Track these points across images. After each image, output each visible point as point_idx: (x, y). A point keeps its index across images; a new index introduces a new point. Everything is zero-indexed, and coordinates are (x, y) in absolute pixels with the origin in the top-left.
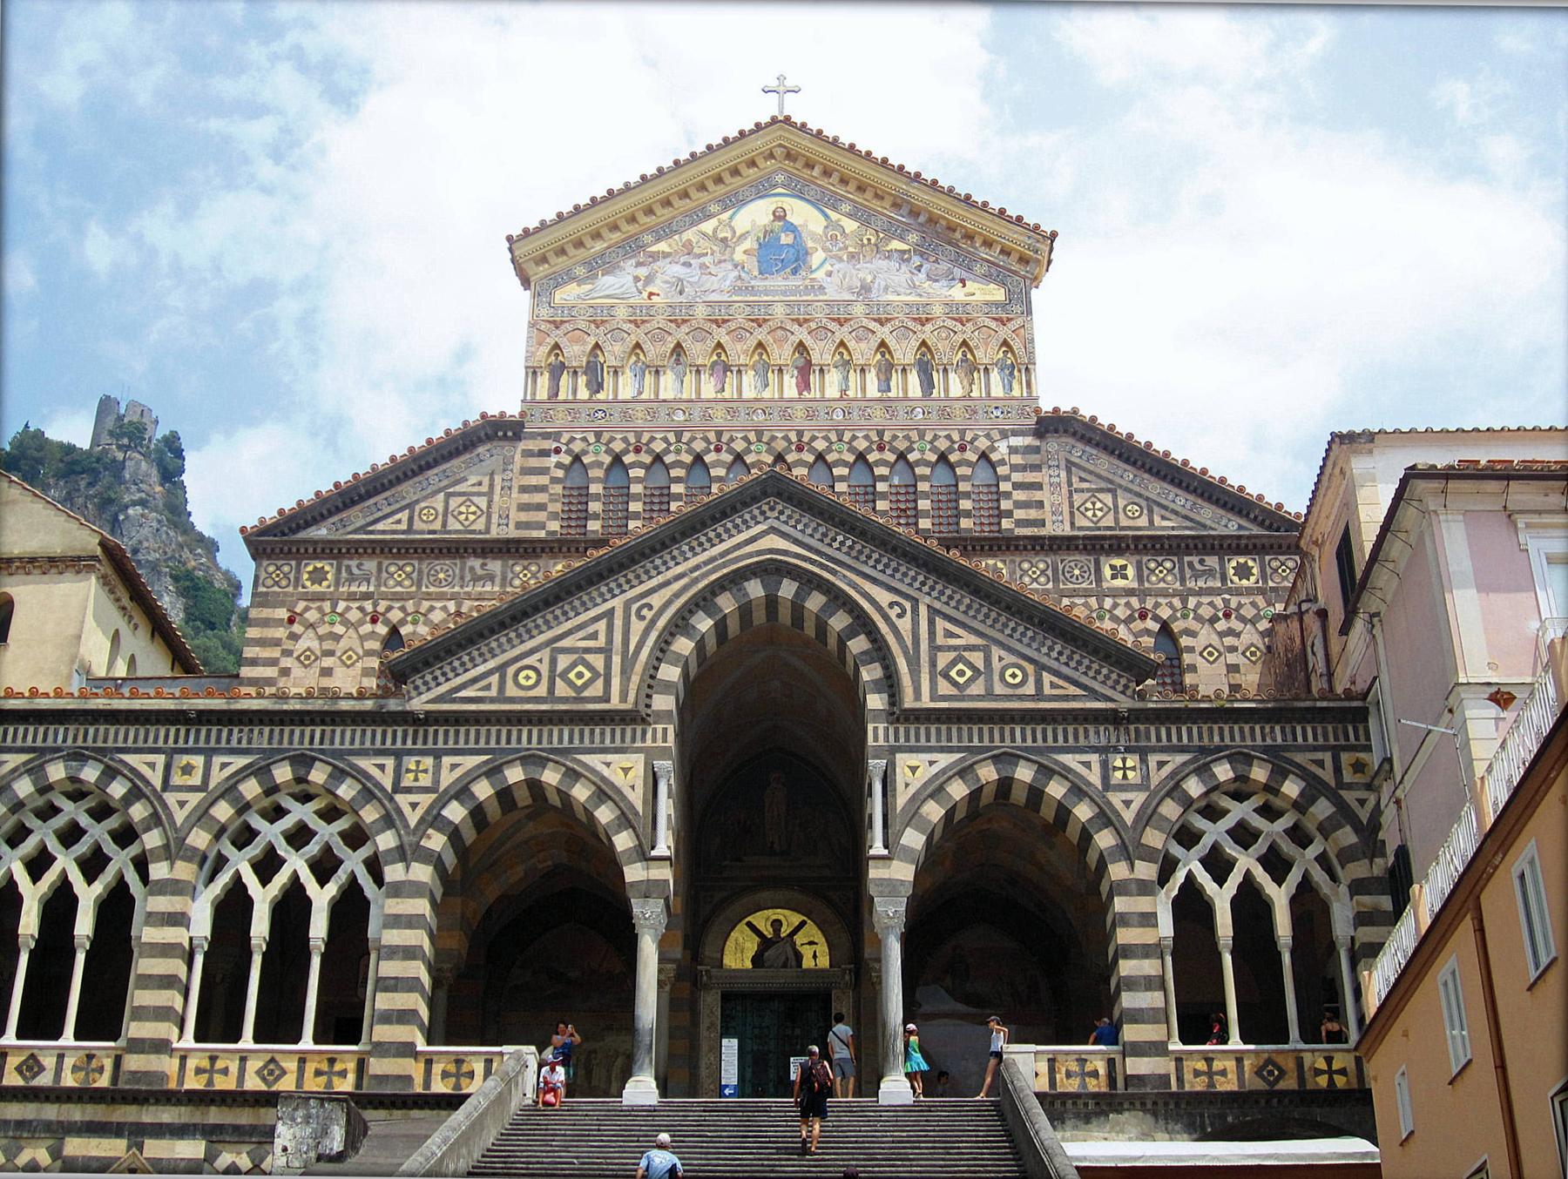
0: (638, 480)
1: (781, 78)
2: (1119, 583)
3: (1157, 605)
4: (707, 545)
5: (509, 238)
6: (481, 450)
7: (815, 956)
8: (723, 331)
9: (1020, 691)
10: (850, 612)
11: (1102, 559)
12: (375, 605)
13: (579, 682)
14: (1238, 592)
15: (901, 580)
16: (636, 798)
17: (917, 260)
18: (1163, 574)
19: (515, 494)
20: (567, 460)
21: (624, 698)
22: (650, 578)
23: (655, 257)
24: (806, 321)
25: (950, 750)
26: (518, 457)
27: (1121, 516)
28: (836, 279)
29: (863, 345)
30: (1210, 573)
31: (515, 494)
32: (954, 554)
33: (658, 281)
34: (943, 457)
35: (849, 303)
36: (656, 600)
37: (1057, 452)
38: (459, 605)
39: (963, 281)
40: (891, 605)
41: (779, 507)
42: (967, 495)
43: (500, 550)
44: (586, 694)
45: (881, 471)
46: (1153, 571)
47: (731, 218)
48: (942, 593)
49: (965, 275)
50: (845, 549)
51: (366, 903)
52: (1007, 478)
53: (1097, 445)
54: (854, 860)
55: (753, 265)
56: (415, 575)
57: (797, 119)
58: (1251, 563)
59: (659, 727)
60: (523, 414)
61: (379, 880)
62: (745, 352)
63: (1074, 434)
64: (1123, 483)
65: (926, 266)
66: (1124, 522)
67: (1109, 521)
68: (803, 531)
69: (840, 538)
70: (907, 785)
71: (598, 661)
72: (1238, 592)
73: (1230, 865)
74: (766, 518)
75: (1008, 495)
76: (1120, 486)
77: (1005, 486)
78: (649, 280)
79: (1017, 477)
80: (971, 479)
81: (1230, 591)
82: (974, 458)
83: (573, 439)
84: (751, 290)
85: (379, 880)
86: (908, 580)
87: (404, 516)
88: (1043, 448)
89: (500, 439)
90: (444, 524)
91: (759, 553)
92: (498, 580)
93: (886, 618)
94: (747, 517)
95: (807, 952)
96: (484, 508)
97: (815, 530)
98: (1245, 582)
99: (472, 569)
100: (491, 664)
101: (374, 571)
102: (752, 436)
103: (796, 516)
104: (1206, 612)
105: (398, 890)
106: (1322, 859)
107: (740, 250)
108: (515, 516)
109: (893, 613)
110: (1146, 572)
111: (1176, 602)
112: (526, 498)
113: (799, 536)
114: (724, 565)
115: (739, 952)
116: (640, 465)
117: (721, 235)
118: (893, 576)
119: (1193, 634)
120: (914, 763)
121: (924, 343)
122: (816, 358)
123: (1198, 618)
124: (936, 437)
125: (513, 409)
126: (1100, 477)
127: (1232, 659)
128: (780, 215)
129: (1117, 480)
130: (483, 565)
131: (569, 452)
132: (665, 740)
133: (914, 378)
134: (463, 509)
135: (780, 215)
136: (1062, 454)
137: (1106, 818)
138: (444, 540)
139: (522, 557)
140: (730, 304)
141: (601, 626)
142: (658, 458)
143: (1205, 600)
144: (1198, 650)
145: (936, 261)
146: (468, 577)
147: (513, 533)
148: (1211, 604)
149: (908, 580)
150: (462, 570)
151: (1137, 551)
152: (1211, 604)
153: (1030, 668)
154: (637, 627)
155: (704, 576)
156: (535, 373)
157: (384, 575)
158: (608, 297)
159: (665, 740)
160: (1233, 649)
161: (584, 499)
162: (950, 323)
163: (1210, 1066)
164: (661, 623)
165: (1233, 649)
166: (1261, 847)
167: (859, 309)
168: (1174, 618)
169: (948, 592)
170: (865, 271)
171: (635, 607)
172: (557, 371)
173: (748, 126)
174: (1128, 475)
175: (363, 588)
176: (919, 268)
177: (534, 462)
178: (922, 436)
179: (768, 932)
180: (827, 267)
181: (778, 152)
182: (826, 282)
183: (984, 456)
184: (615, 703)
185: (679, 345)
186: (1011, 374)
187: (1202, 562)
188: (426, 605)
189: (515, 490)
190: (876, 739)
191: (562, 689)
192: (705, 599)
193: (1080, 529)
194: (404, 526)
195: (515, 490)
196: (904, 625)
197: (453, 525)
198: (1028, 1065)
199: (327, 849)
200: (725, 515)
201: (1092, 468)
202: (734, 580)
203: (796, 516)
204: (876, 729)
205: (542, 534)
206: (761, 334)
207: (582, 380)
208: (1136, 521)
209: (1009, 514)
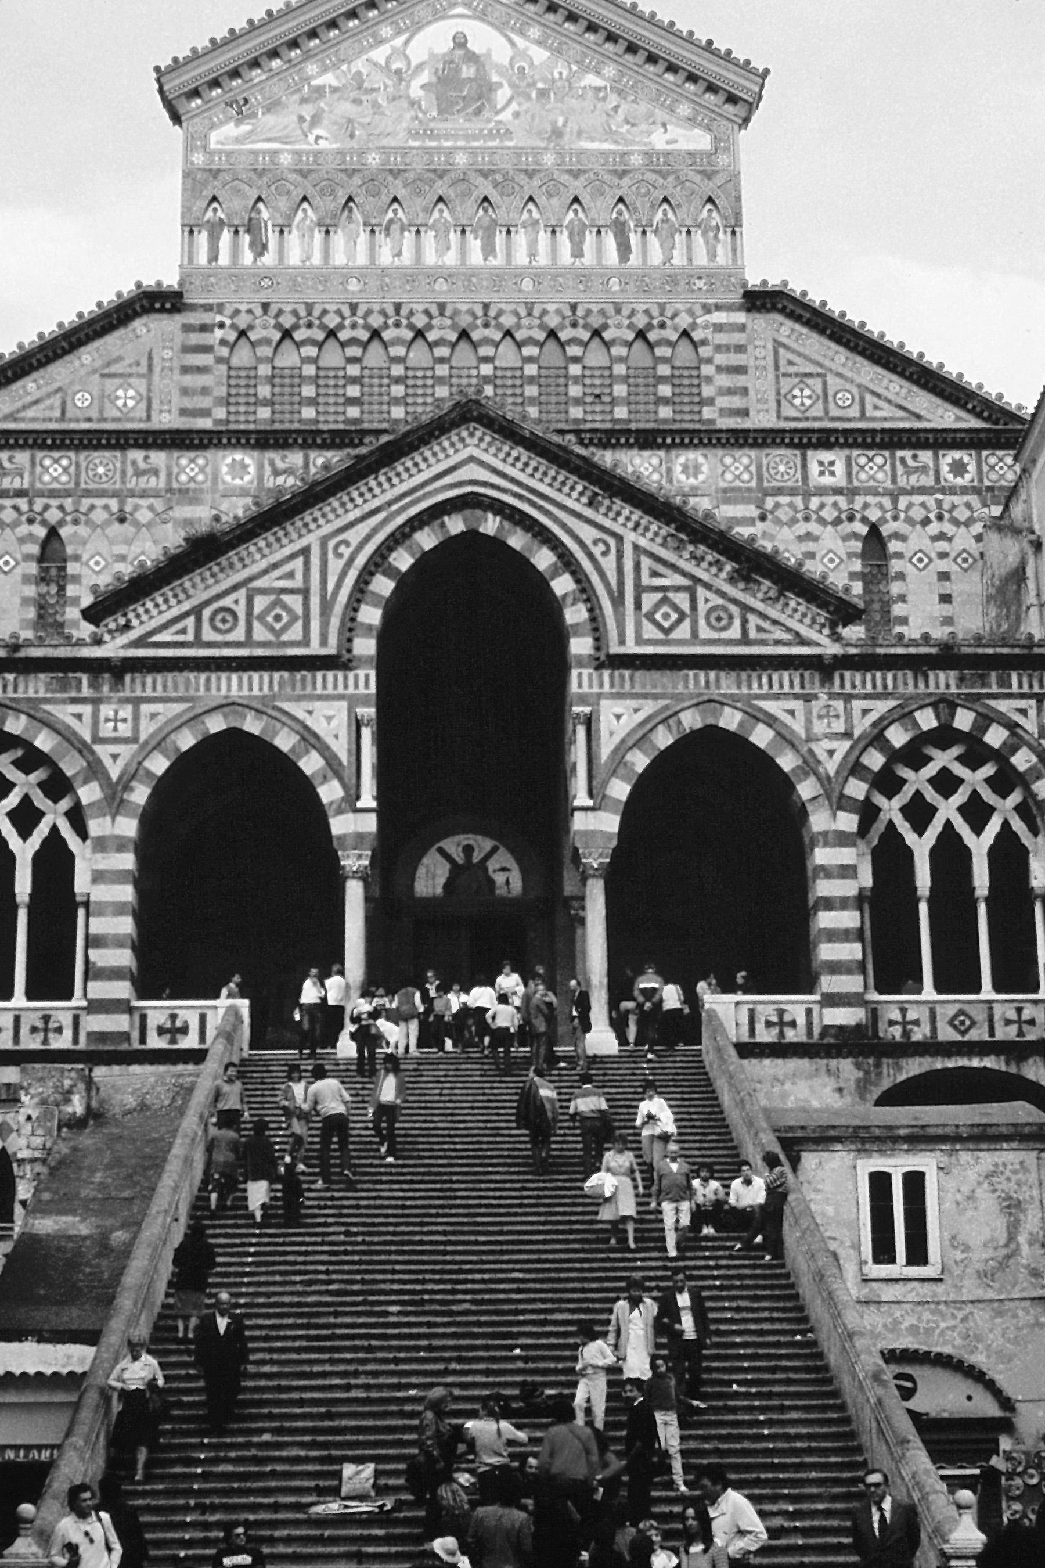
2: (827, 480)
3: (866, 506)
4: (405, 476)
7: (508, 882)
8: (398, 182)
9: (724, 635)
10: (553, 549)
11: (810, 453)
12: (31, 503)
13: (278, 626)
14: (952, 491)
16: (341, 749)
17: (613, 99)
18: (874, 468)
19: (177, 376)
20: (232, 336)
21: (324, 642)
23: (319, 91)
25: (655, 697)
27: (832, 406)
29: (555, 201)
30: (924, 469)
33: (325, 122)
34: (641, 335)
35: (536, 152)
39: (664, 125)
40: (595, 542)
41: (478, 434)
44: (285, 638)
46: (862, 468)
49: (666, 117)
51: (71, 857)
54: (557, 809)
56: (72, 469)
58: (966, 459)
59: (361, 673)
60: (181, 284)
61: (82, 833)
63: (782, 311)
65: (624, 107)
66: (834, 412)
67: (817, 411)
70: (611, 734)
71: (295, 602)
72: (952, 491)
73: (932, 811)
77: (707, 370)
79: (720, 359)
81: (943, 491)
82: (674, 337)
83: (237, 312)
85: (82, 833)
87: (56, 401)
88: (749, 326)
90: (101, 411)
92: (163, 475)
93: (591, 556)
95: (499, 878)
98: (959, 481)
99: (134, 463)
100: (186, 606)
101: (27, 465)
102: (434, 311)
104: (918, 514)
105: (101, 845)
106: (1022, 810)
108: (178, 402)
109: (597, 550)
110: (855, 469)
111: (886, 502)
115: (431, 878)
117: (394, 67)
119: (903, 538)
120: (618, 710)
123: (910, 521)
124: (633, 313)
126: (807, 358)
127: (943, 565)
128: (460, 42)
129: (827, 363)
130: (146, 458)
131: (233, 326)
132: (367, 686)
133: (610, 241)
135: (460, 42)
136: (770, 334)
137: (810, 766)
140: (405, 151)
141: (299, 563)
142: (332, 334)
143: (918, 499)
144: (908, 555)
146: (130, 471)
148: (923, 505)
150: (123, 463)
151: (847, 445)
152: (923, 505)
153: (734, 609)
154: (335, 566)
155: (403, 509)
156: (191, 232)
157: (38, 469)
159: (367, 686)
160: (943, 555)
162: (651, 177)
163: (904, 1016)
164: (361, 560)
165: (943, 555)
166: (960, 797)
167: (549, 159)
168: (883, 520)
172: (215, 230)
174: (839, 357)
175: (17, 484)
177: (195, 338)
178: (618, 311)
179: (460, 859)
180: (514, 106)
183: (685, 334)
184: (315, 648)
185: (350, 199)
186: (716, 236)
187: (915, 457)
188: (86, 502)
190: (580, 686)
191: (260, 633)
193: (787, 419)
194: (57, 414)
195: (177, 371)
196: (609, 563)
198: (727, 1010)
199: (26, 800)
201: (801, 350)
204: (580, 675)
206: (441, 188)
207: (246, 239)
208: (845, 410)
209: (711, 402)
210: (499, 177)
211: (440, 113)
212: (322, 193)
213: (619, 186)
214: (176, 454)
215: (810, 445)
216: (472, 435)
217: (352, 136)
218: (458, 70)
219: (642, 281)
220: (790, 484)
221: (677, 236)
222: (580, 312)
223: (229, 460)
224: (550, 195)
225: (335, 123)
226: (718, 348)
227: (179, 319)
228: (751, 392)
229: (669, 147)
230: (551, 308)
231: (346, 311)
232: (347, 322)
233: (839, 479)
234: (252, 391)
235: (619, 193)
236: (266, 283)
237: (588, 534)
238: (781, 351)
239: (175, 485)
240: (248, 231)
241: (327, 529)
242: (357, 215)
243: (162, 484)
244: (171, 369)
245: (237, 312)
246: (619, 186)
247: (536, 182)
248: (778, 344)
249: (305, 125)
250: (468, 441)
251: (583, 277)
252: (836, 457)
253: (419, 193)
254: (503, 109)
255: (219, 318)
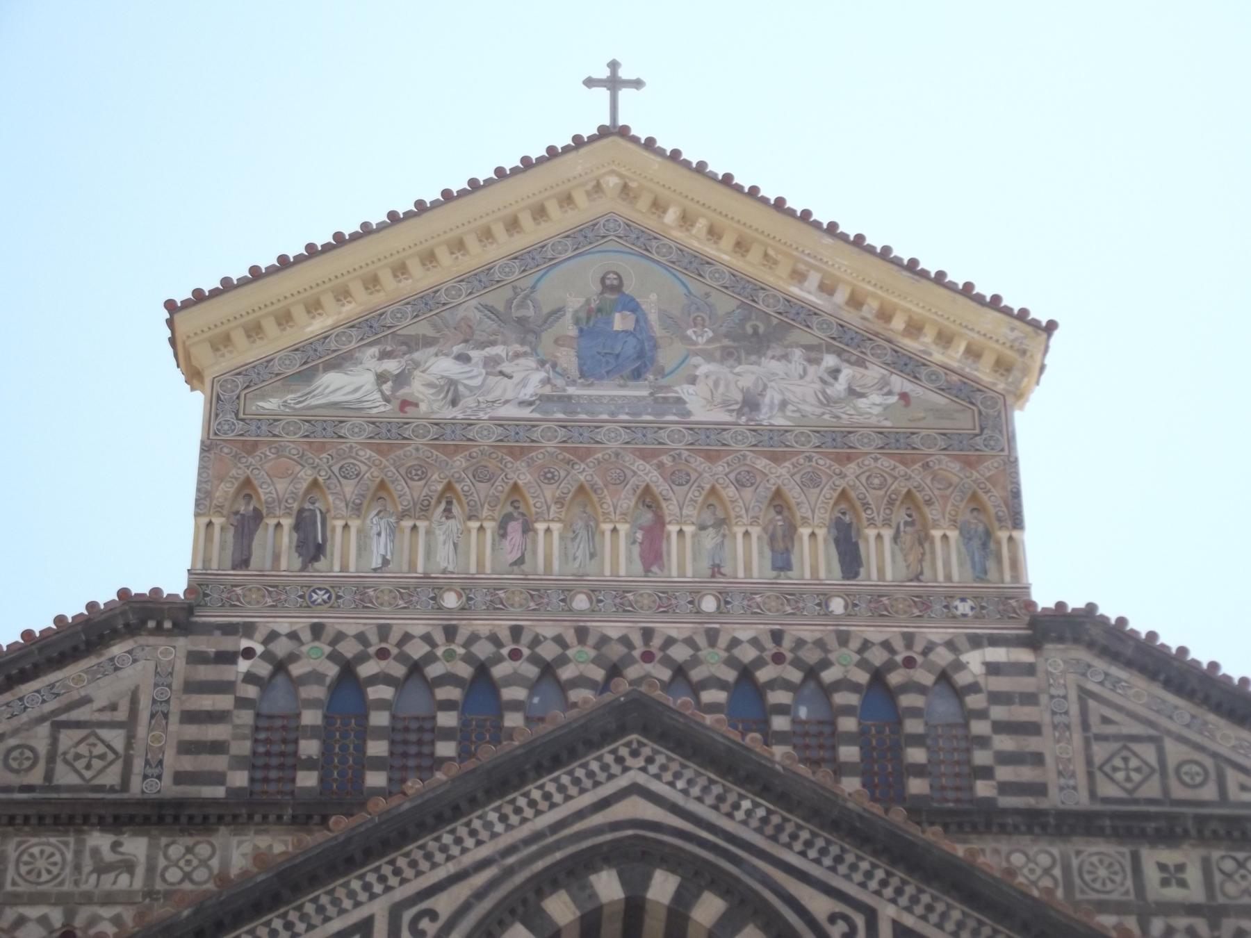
0: (382, 704)
1: (614, 65)
4: (529, 813)
5: (170, 305)
6: (117, 650)
15: (848, 877)
17: (830, 360)
19: (174, 725)
20: (264, 669)
22: (434, 866)
24: (654, 454)
26: (181, 666)
27: (1173, 783)
28: (702, 388)
29: (748, 493)
31: (174, 725)
32: (932, 835)
35: (722, 428)
36: (445, 904)
37: (1064, 672)
38: (70, 915)
39: (904, 396)
41: (646, 751)
42: (917, 740)
43: (146, 820)
45: (779, 697)
47: (533, 287)
48: (914, 900)
49: (908, 387)
50: (754, 823)
52: (982, 714)
53: (1129, 664)
55: (568, 359)
57: (640, 131)
62: (560, 502)
63: (1091, 645)
64: (1173, 727)
66: (1178, 792)
68: (685, 792)
69: (746, 804)
74: (626, 769)
75: (983, 742)
76: (1169, 733)
78: (401, 379)
79: (998, 712)
80: (921, 711)
82: (927, 679)
84: (565, 401)
86: (858, 877)
88: (1041, 666)
89: (153, 633)
91: (615, 826)
92: (140, 871)
94: (595, 766)
96: (119, 745)
97: (706, 790)
102: (570, 637)
103: (675, 767)
107: (547, 337)
108: (172, 761)
112: (193, 732)
113: (679, 799)
114: (557, 846)
116: (383, 679)
117: (515, 313)
118: (833, 869)
121: (843, 495)
122: (670, 509)
125: (175, 584)
128: (612, 286)
129: (1164, 722)
134: (83, 749)
135: (612, 286)
136: (1072, 679)
138: (48, 802)
139: (183, 832)
140: (531, 425)
142: (416, 668)
145: (861, 363)
147: (167, 788)
149: (858, 877)
158: (335, 405)
161: (291, 736)
162: (886, 463)
169: (925, 898)
170: (747, 375)
171: (408, 915)
173: (562, 140)
176: (835, 373)
177: (207, 673)
181: (612, 182)
182: (685, 391)
183: (944, 677)
185: (449, 487)
186: (985, 545)
189: (174, 718)
192: (524, 902)
193: (1106, 800)
195: (174, 718)
197: (65, 776)
200: (557, 762)
202: (572, 873)
203: (675, 767)
205: (219, 792)
206: (583, 473)
209: (986, 772)
210: (665, 459)
211: (582, 375)
212: (409, 476)
213: (842, 475)
214: (164, 840)
215: (1143, 836)
216: (635, 754)
217: (454, 403)
218: (610, 323)
219: (879, 605)
220: (1115, 896)
221: (927, 545)
222: (787, 643)
223: (247, 848)
224: (740, 484)
225: (430, 385)
226: (996, 698)
227: (183, 644)
228: (1049, 760)
229: (913, 425)
230: (744, 634)
231: (439, 637)
232: (440, 652)
233: (1195, 893)
234: (290, 748)
235: (842, 483)
236: (319, 597)
237: (820, 905)
238: (1092, 703)
239: (159, 886)
240: (297, 527)
241: (400, 893)
242: (456, 509)
243: (138, 884)
244: (166, 716)
245: (273, 636)
246: (842, 475)
247: (720, 468)
248: (1085, 694)
249: (387, 387)
250: (630, 762)
251: (792, 597)
252: (1188, 857)
253: (548, 477)
254: (672, 372)
255: (245, 643)
